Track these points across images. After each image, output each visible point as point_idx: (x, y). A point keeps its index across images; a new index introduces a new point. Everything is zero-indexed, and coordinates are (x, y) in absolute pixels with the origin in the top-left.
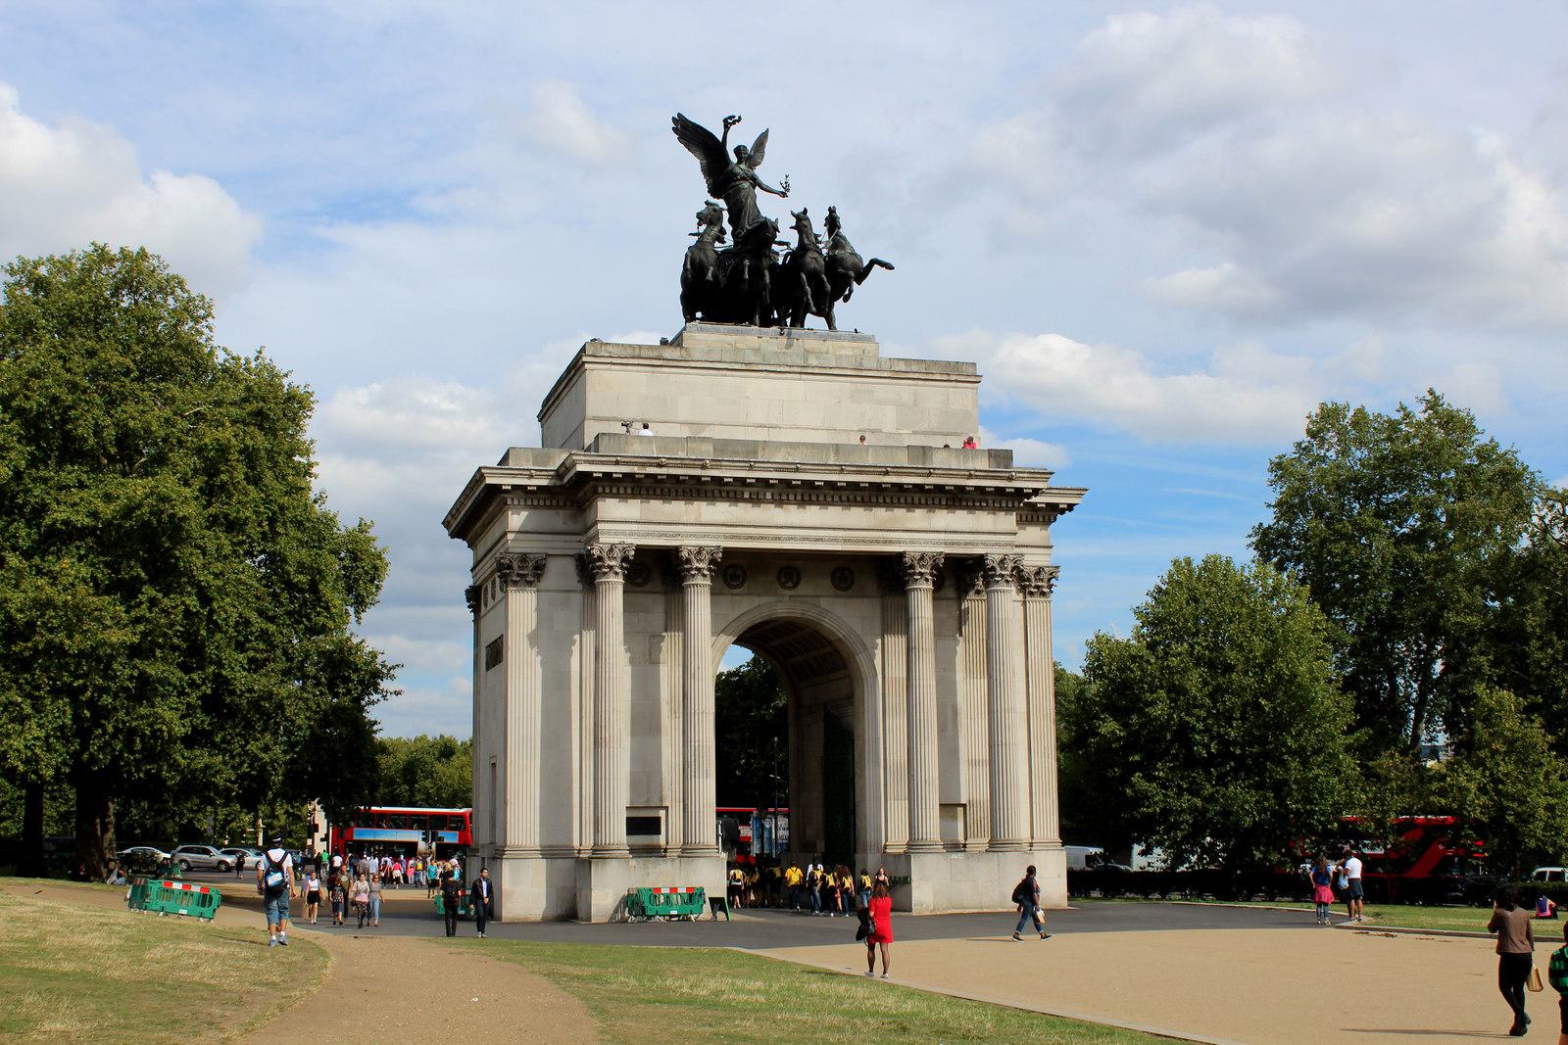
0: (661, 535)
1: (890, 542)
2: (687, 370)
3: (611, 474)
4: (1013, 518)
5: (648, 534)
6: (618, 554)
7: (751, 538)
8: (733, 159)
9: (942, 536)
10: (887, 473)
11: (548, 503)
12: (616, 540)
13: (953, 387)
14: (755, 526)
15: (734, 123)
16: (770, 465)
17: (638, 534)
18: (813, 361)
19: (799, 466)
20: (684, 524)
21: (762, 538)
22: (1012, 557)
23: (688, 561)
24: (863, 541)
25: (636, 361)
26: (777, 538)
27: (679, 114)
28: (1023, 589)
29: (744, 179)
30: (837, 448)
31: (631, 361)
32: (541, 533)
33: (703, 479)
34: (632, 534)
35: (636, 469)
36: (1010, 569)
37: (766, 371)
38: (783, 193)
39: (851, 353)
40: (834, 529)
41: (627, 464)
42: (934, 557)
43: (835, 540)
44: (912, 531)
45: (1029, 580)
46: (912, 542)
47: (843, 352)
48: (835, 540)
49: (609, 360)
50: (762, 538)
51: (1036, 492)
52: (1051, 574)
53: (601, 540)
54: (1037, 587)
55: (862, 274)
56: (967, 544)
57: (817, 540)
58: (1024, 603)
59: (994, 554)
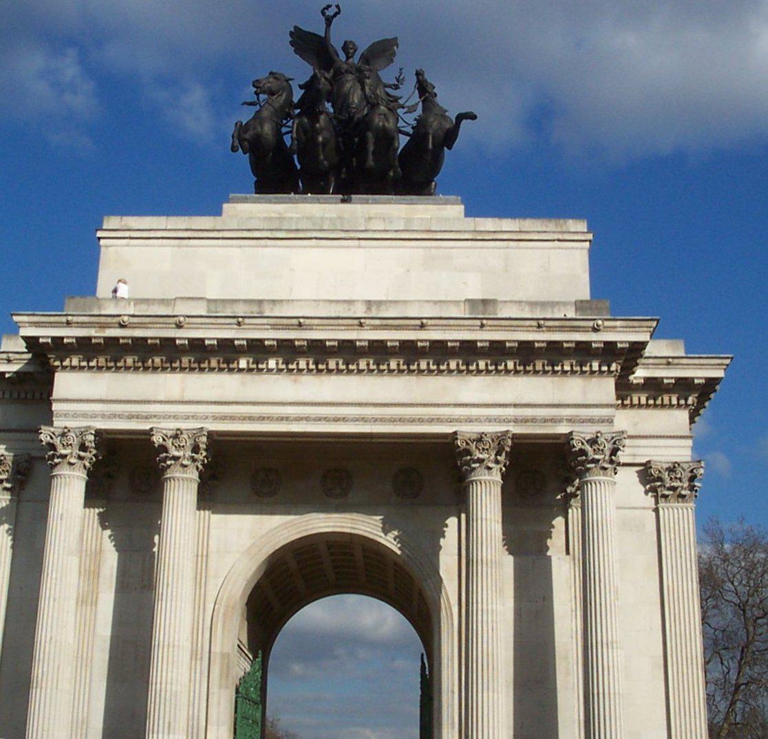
0: (131, 417)
1: (439, 420)
2: (220, 242)
3: (62, 338)
4: (610, 383)
5: (114, 416)
6: (73, 439)
7: (251, 418)
8: (342, 56)
9: (510, 412)
10: (422, 326)
11: (37, 395)
12: (71, 424)
13: (555, 248)
14: (254, 403)
15: (335, 15)
16: (265, 321)
17: (103, 416)
18: (376, 225)
19: (302, 320)
20: (161, 402)
21: (262, 419)
22: (609, 437)
23: (164, 449)
24: (401, 420)
25: (159, 234)
26: (282, 419)
27: (296, 27)
28: (654, 490)
29: (347, 71)
30: (369, 303)
31: (152, 234)
32: (25, 431)
33: (178, 342)
34: (94, 416)
35: (92, 332)
36: (608, 453)
37: (316, 238)
38: (395, 85)
39: (429, 217)
40: (360, 405)
41: (82, 325)
42: (500, 438)
43: (364, 420)
44: (466, 405)
45: (660, 479)
46: (470, 420)
47: (416, 216)
48: (364, 420)
49: (127, 234)
50: (262, 419)
51: (636, 350)
52: (692, 471)
53: (56, 424)
54: (674, 489)
55: (449, 137)
56: (546, 421)
57: (336, 420)
58: (656, 510)
59: (583, 433)
